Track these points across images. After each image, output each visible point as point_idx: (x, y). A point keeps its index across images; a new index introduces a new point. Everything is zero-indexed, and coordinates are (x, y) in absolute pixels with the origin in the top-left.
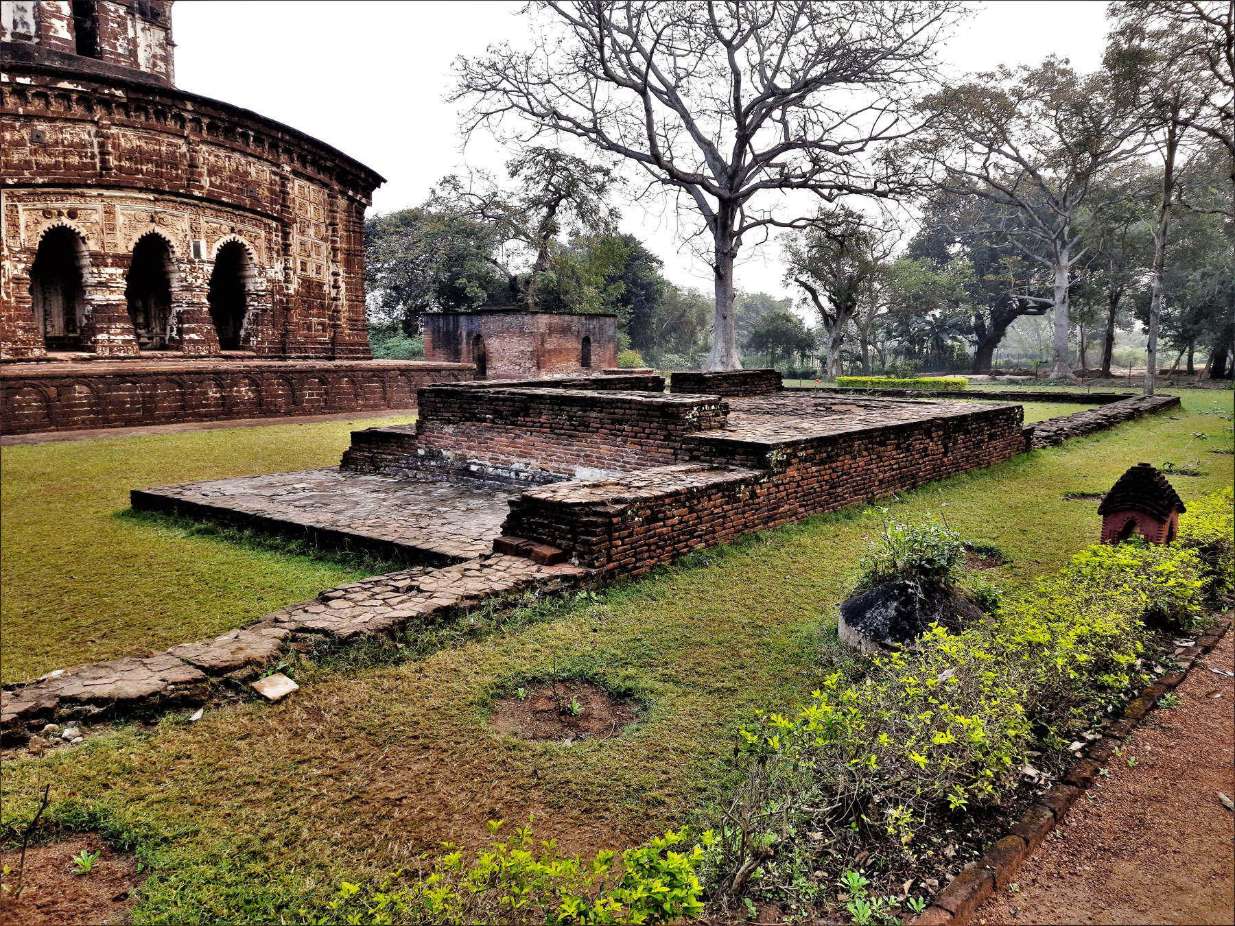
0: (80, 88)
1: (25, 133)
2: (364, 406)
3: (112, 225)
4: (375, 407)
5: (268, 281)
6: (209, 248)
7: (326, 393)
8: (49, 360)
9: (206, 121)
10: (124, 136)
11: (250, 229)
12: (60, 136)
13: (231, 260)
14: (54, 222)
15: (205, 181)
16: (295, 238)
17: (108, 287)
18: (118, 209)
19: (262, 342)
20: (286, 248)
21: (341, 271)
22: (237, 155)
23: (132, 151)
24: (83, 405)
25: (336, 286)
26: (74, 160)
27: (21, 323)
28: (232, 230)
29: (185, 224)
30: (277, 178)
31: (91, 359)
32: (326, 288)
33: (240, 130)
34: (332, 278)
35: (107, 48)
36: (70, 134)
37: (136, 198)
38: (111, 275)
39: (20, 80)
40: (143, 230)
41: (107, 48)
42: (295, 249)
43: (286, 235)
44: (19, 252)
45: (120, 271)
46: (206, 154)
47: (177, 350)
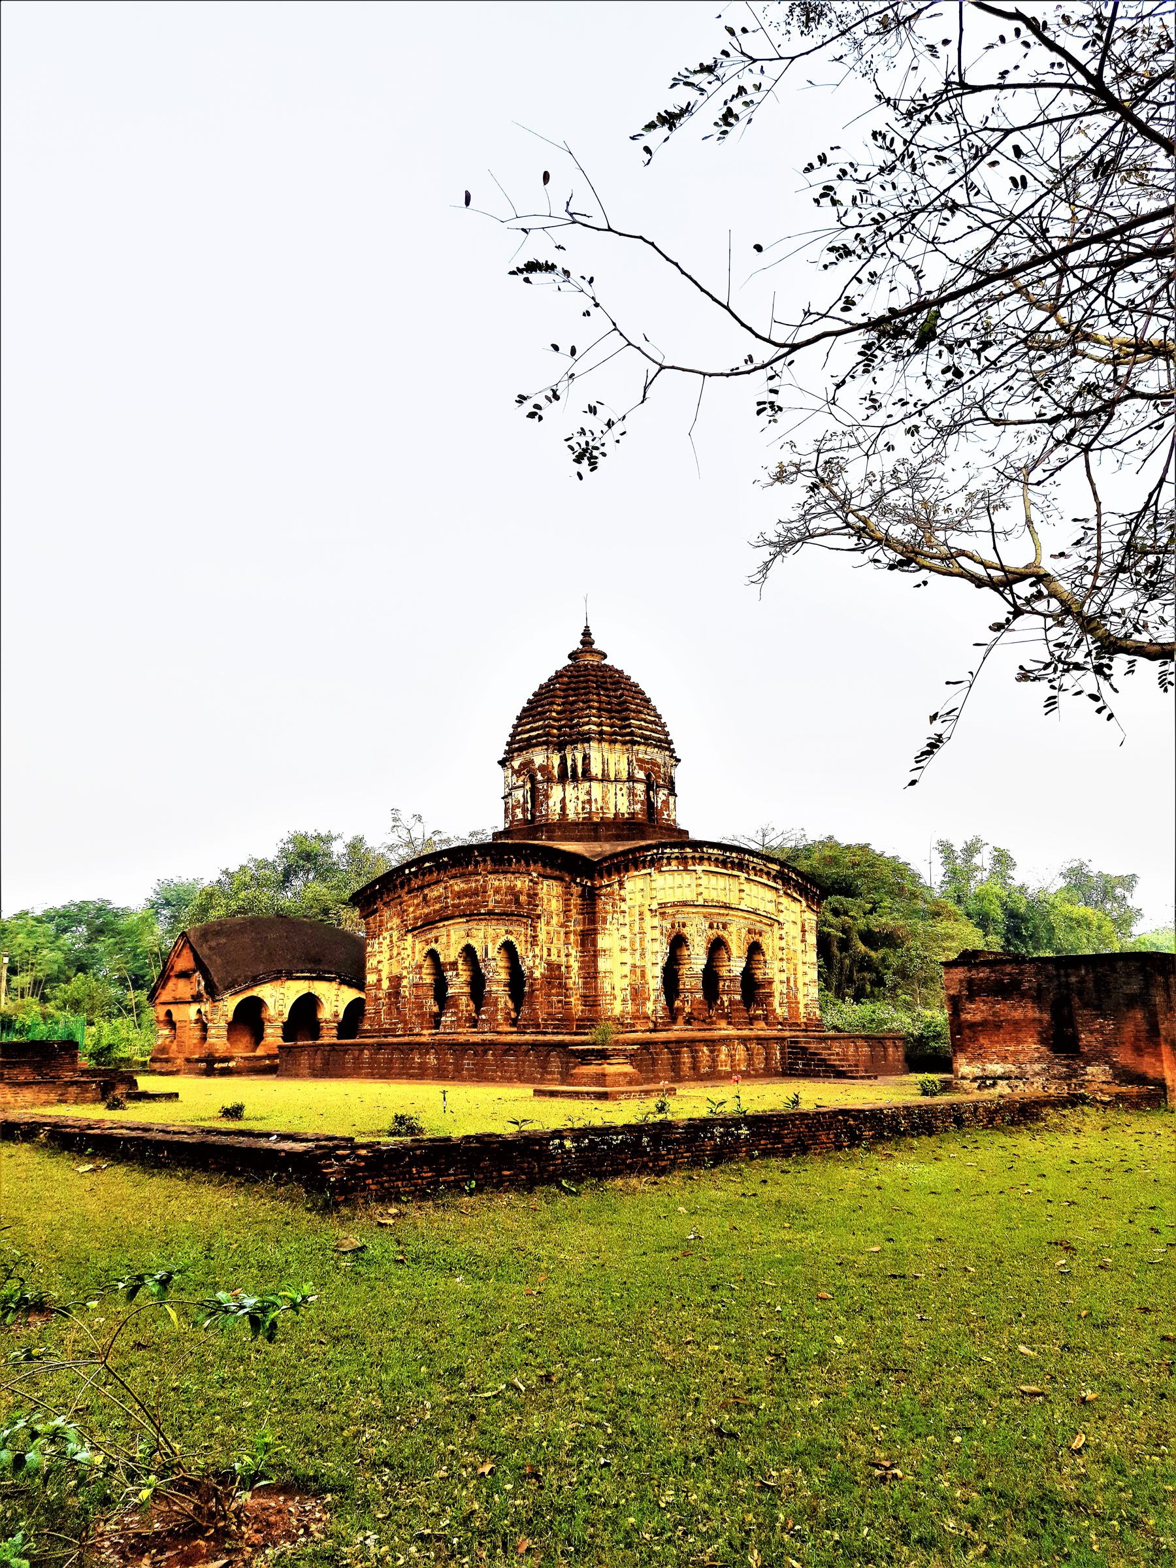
2: (501, 1077)
4: (510, 1080)
18: (452, 932)
20: (534, 937)
21: (573, 952)
22: (509, 875)
28: (507, 932)
29: (481, 934)
31: (436, 1034)
40: (463, 943)
42: (542, 936)
43: (535, 928)
46: (494, 881)
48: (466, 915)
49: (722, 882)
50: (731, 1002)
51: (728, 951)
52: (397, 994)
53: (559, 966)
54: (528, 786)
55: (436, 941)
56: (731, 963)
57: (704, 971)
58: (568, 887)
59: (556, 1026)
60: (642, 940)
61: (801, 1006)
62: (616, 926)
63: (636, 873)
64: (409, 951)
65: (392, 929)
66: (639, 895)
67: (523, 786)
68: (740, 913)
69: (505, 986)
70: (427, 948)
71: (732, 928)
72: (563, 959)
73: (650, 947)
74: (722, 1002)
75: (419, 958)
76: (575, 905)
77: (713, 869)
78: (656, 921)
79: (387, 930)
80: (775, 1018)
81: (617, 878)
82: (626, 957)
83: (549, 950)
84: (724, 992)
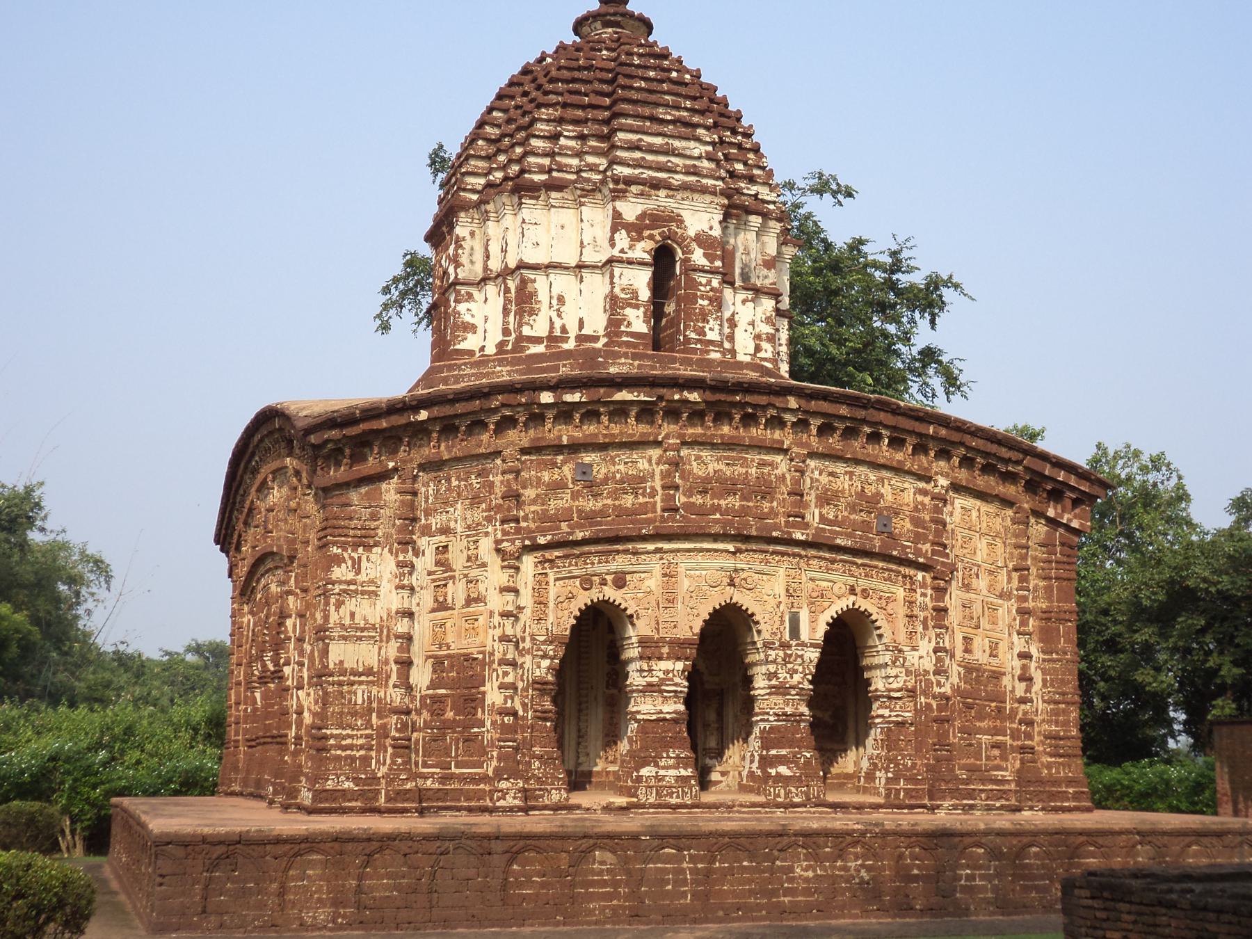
0: (642, 398)
1: (567, 471)
3: (669, 594)
5: (908, 673)
6: (813, 621)
7: (998, 875)
8: (571, 808)
10: (698, 458)
11: (880, 586)
12: (613, 469)
13: (846, 640)
14: (595, 595)
15: (813, 515)
16: (954, 598)
17: (661, 691)
18: (682, 568)
19: (896, 779)
20: (941, 612)
21: (1034, 651)
22: (861, 470)
23: (707, 480)
24: (604, 884)
25: (1026, 678)
26: (628, 501)
27: (537, 750)
28: (852, 591)
30: (927, 500)
32: (1006, 681)
33: (868, 430)
34: (1017, 663)
35: (693, 335)
36: (623, 464)
37: (708, 550)
38: (667, 672)
39: (568, 398)
40: (716, 600)
41: (693, 335)
42: (954, 616)
43: (940, 592)
44: (544, 643)
45: (680, 665)
47: (758, 794)
52: (470, 701)
53: (997, 676)
55: (620, 582)
59: (991, 795)
64: (526, 599)
65: (446, 531)
70: (583, 599)
75: (562, 620)
76: (1035, 558)
79: (427, 531)
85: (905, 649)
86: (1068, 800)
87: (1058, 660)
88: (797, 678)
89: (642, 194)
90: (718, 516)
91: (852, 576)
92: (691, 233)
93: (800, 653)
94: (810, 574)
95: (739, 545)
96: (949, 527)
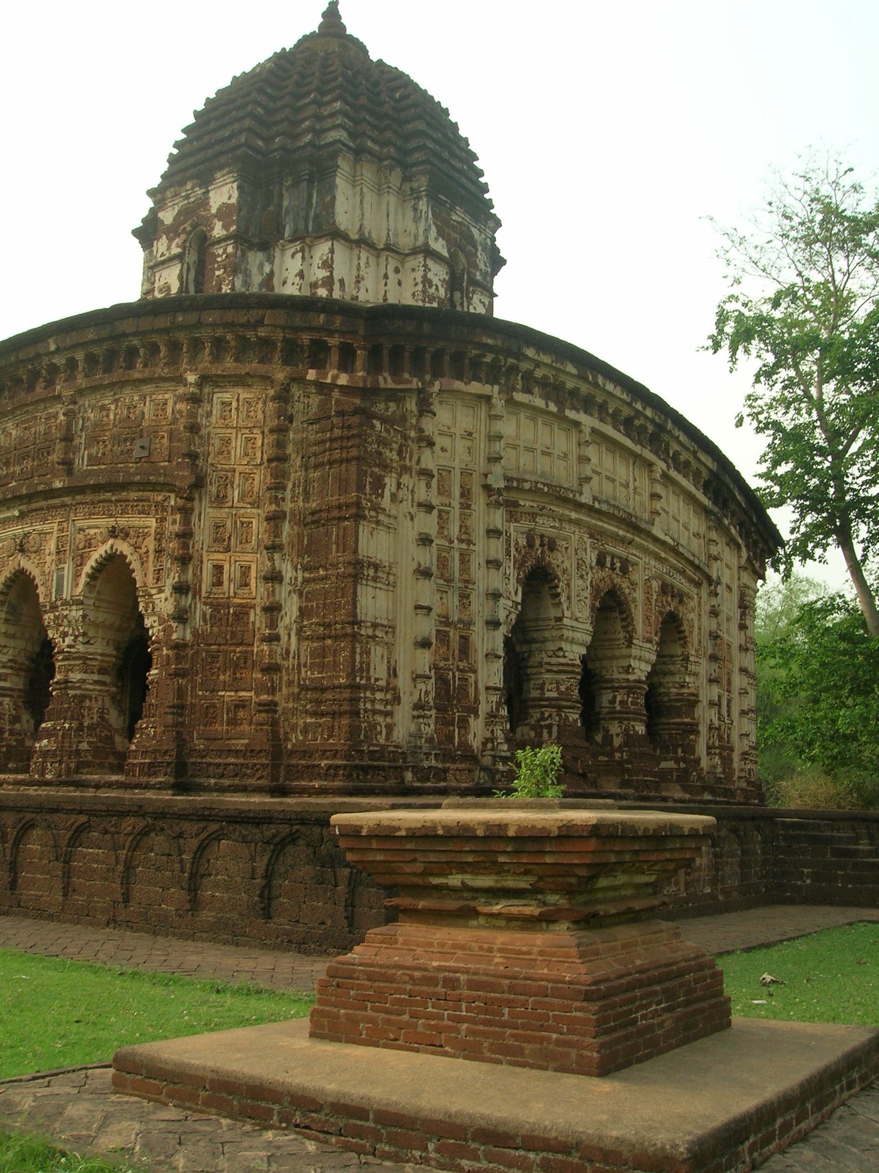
9: (80, 356)
16: (206, 517)
21: (288, 571)
22: (127, 391)
25: (273, 610)
28: (113, 533)
48: (19, 499)
49: (622, 471)
50: (630, 739)
51: (628, 620)
54: (191, 258)
56: (634, 652)
57: (584, 660)
58: (283, 397)
60: (465, 559)
61: (736, 756)
62: (406, 507)
63: (458, 385)
66: (461, 446)
67: (180, 257)
68: (652, 547)
69: (102, 671)
71: (638, 576)
72: (258, 591)
73: (485, 579)
74: (608, 738)
76: (300, 444)
77: (608, 430)
78: (498, 518)
80: (700, 778)
81: (416, 383)
82: (426, 592)
83: (218, 569)
84: (613, 715)
85: (153, 591)
86: (319, 777)
87: (326, 578)
88: (69, 640)
89: (176, 195)
90: (14, 484)
91: (111, 516)
92: (214, 211)
93: (65, 613)
94: (79, 524)
95: (24, 508)
96: (204, 431)
